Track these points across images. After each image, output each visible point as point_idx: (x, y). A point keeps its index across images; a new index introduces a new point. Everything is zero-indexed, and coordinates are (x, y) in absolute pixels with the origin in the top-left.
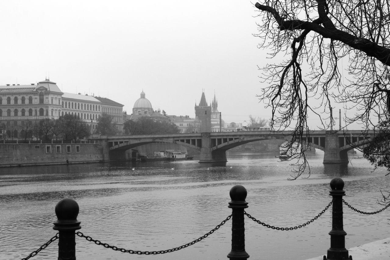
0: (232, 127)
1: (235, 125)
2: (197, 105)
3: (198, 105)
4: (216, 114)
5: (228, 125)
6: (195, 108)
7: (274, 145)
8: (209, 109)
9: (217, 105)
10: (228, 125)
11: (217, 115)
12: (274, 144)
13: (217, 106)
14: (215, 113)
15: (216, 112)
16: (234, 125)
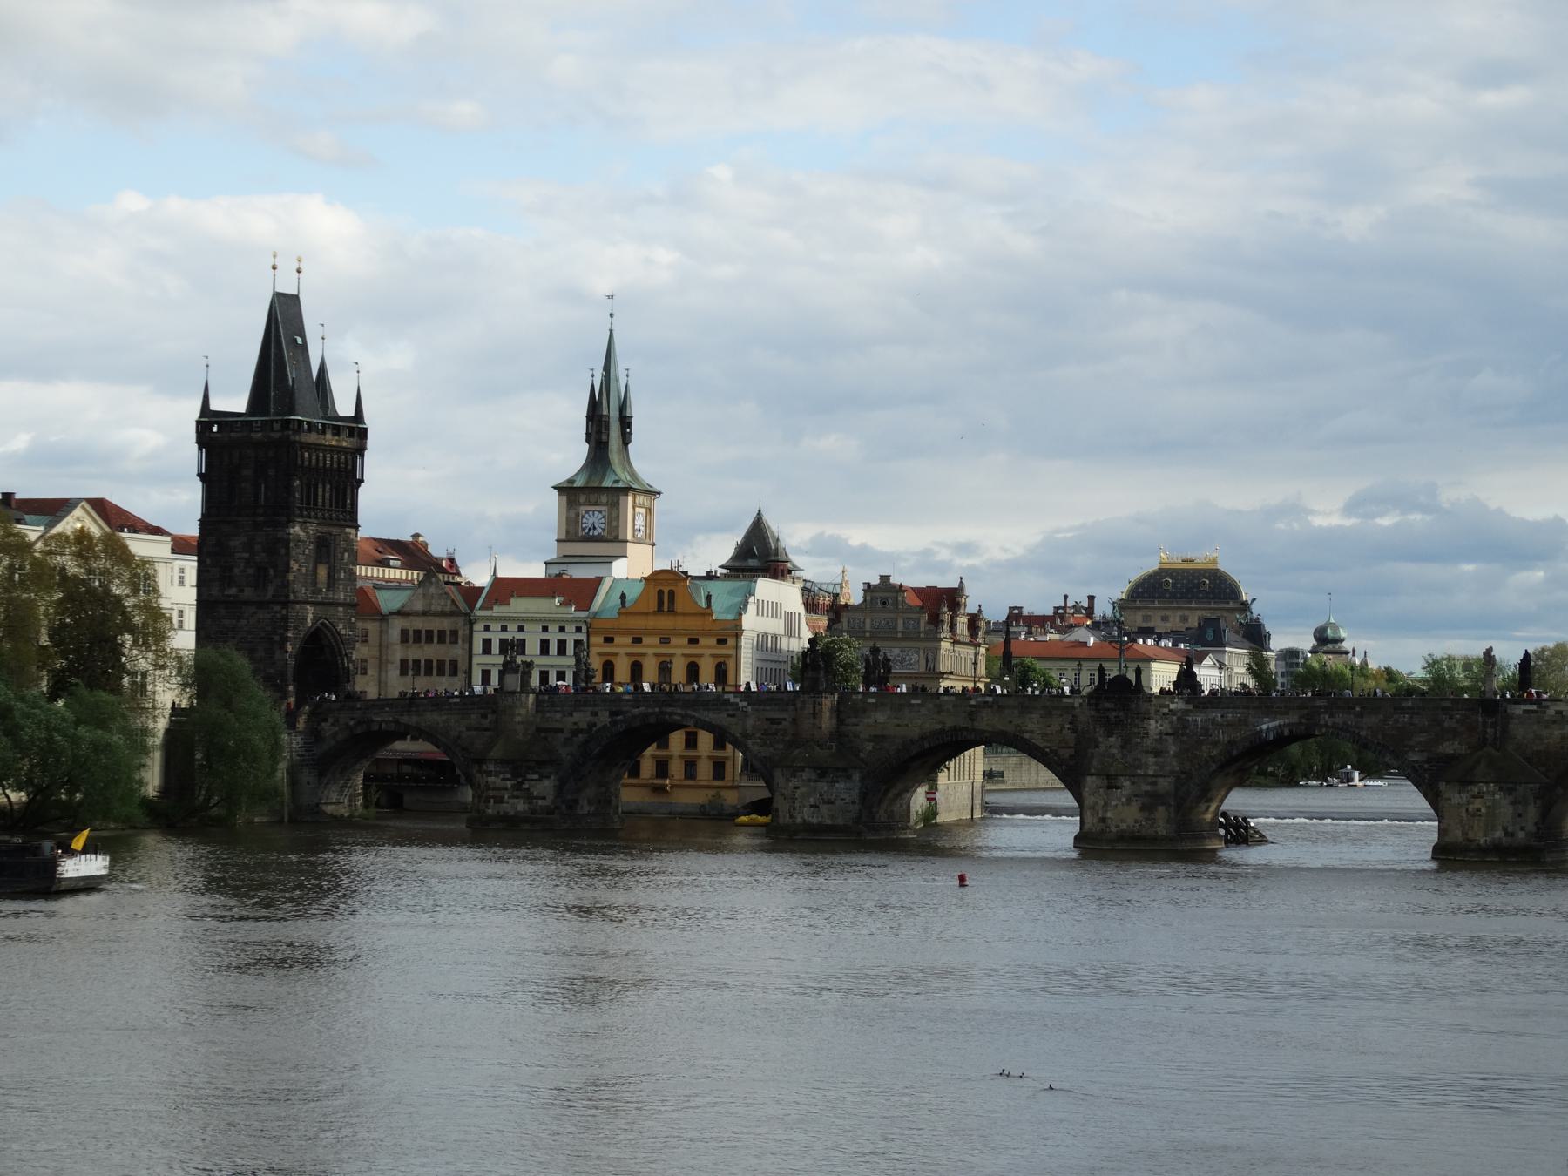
0: (653, 606)
1: (678, 590)
2: (215, 406)
3: (234, 400)
4: (604, 498)
5: (623, 596)
6: (203, 427)
7: (823, 786)
8: (330, 440)
9: (625, 422)
10: (623, 596)
11: (615, 506)
12: (822, 772)
13: (626, 439)
14: (601, 490)
15: (607, 483)
16: (671, 594)
